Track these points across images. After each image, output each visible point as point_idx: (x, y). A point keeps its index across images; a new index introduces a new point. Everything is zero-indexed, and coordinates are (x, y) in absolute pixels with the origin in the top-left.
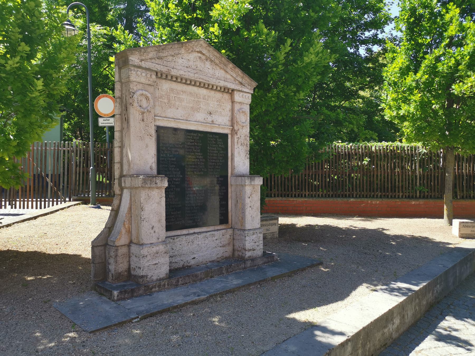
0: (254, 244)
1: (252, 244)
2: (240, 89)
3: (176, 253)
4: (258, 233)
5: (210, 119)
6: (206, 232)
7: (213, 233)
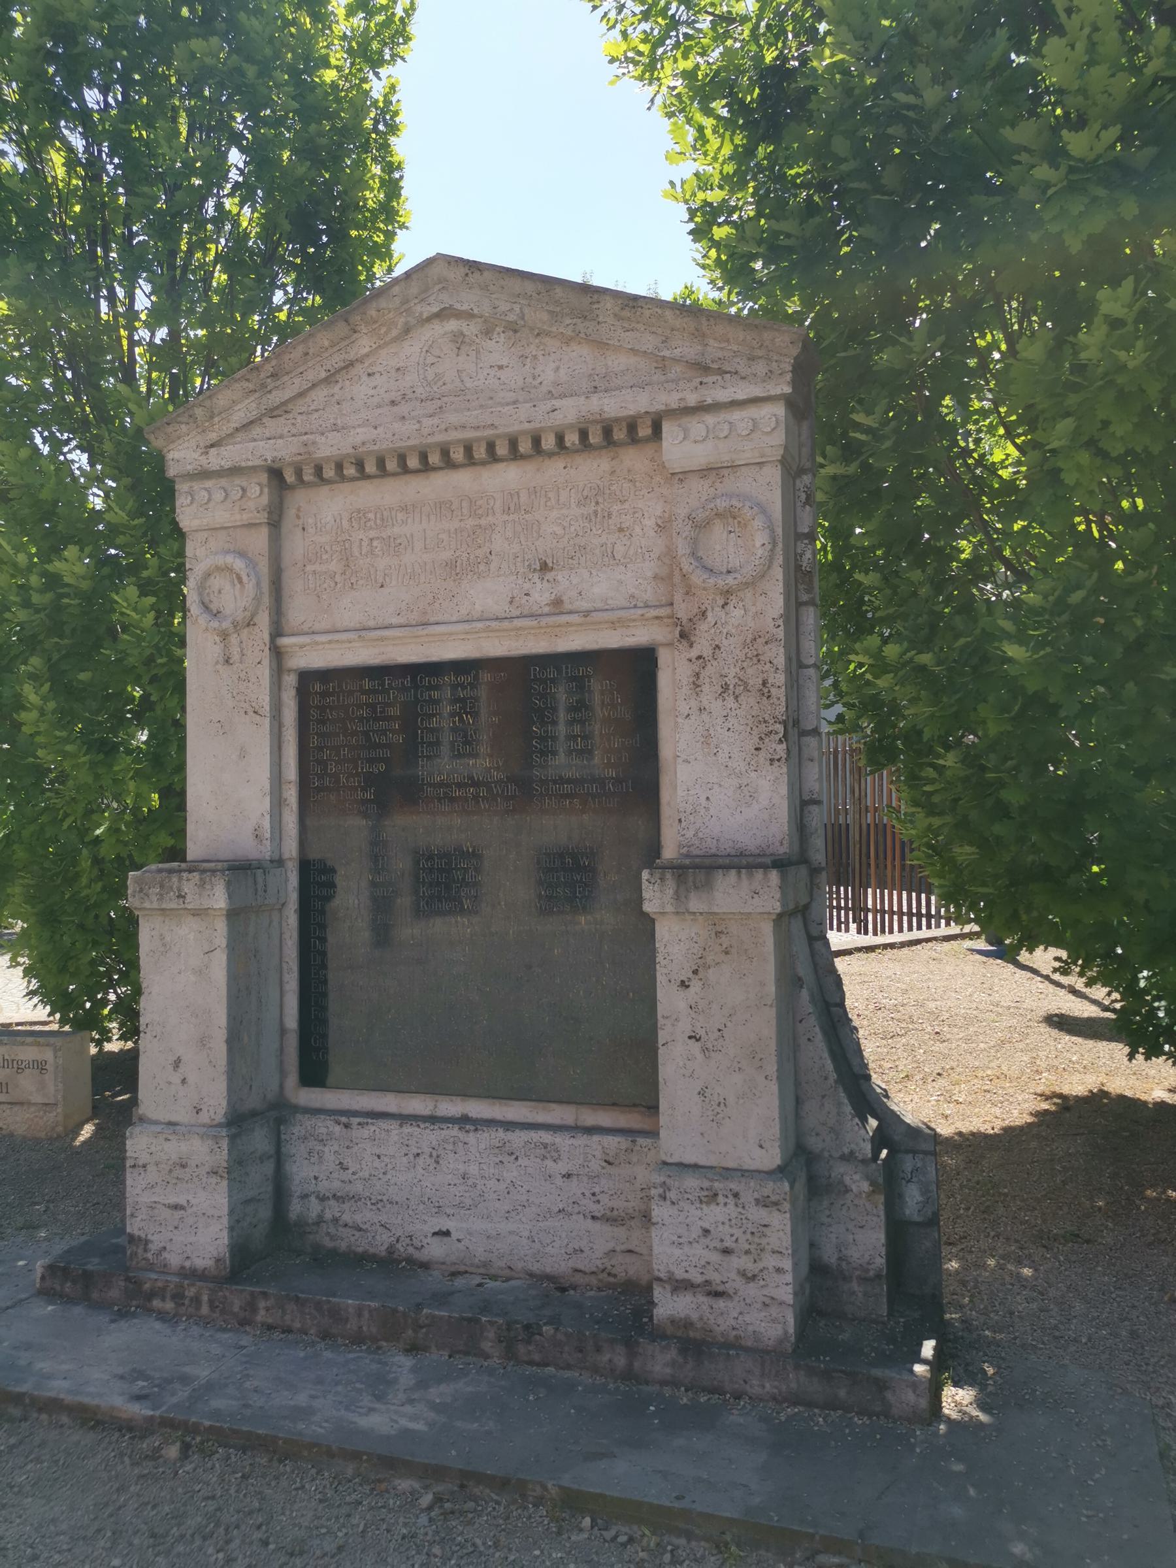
0: (715, 1257)
1: (699, 1253)
2: (692, 399)
3: (358, 1187)
4: (748, 1197)
5: (541, 595)
6: (509, 1126)
7: (546, 1137)
